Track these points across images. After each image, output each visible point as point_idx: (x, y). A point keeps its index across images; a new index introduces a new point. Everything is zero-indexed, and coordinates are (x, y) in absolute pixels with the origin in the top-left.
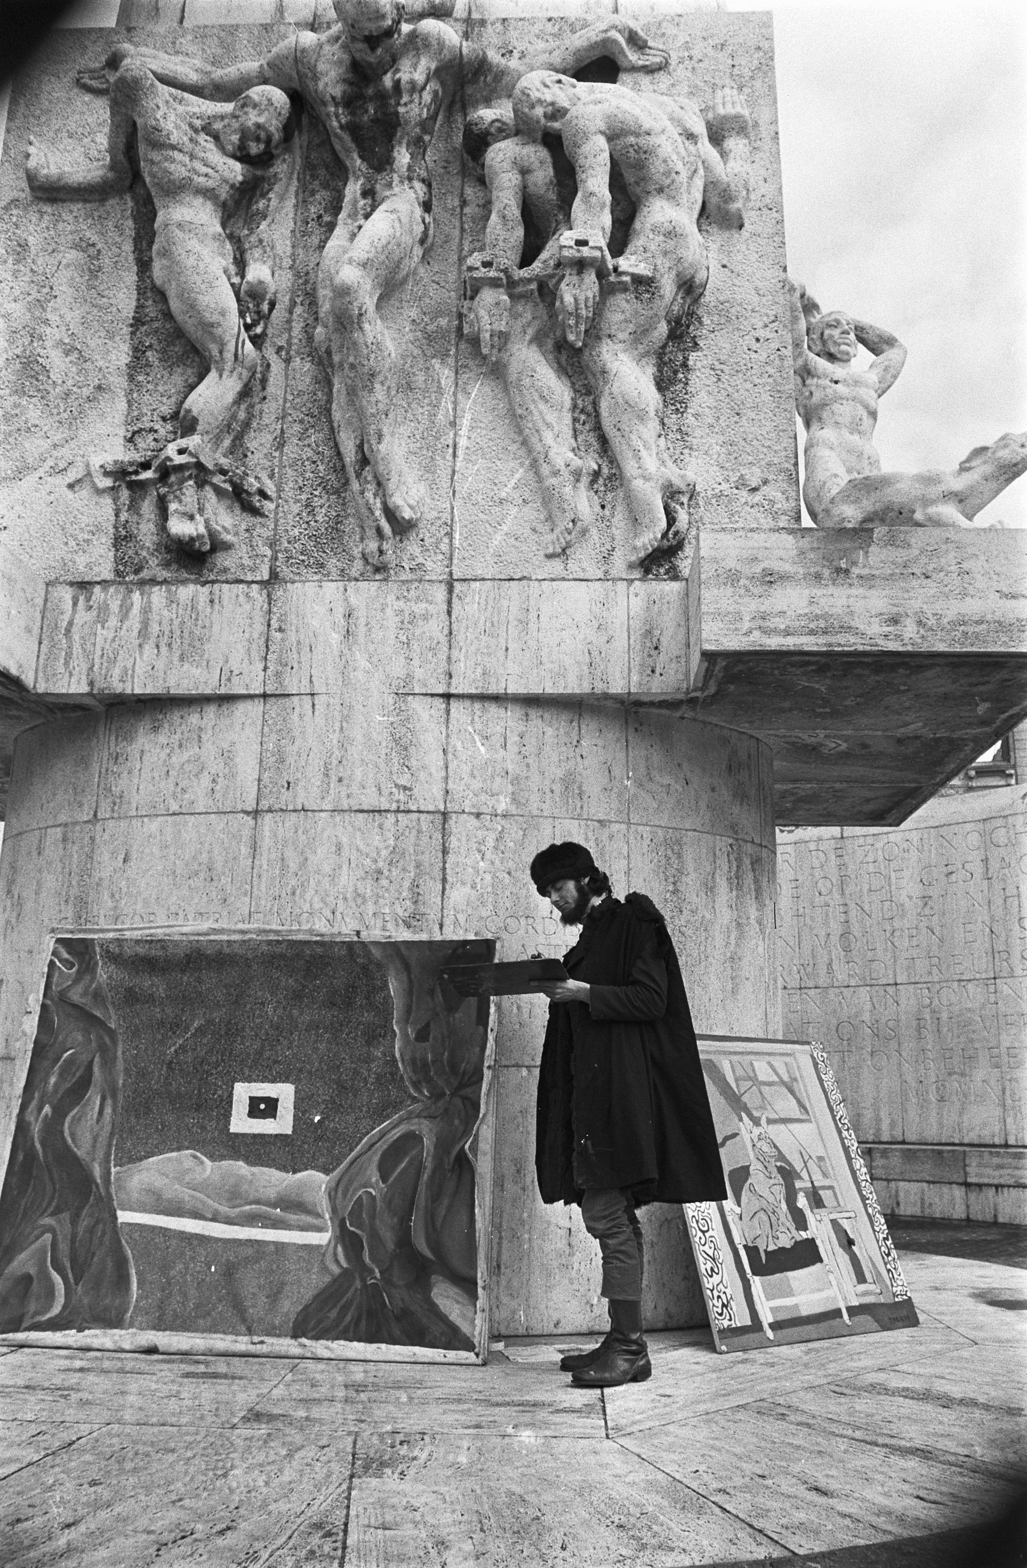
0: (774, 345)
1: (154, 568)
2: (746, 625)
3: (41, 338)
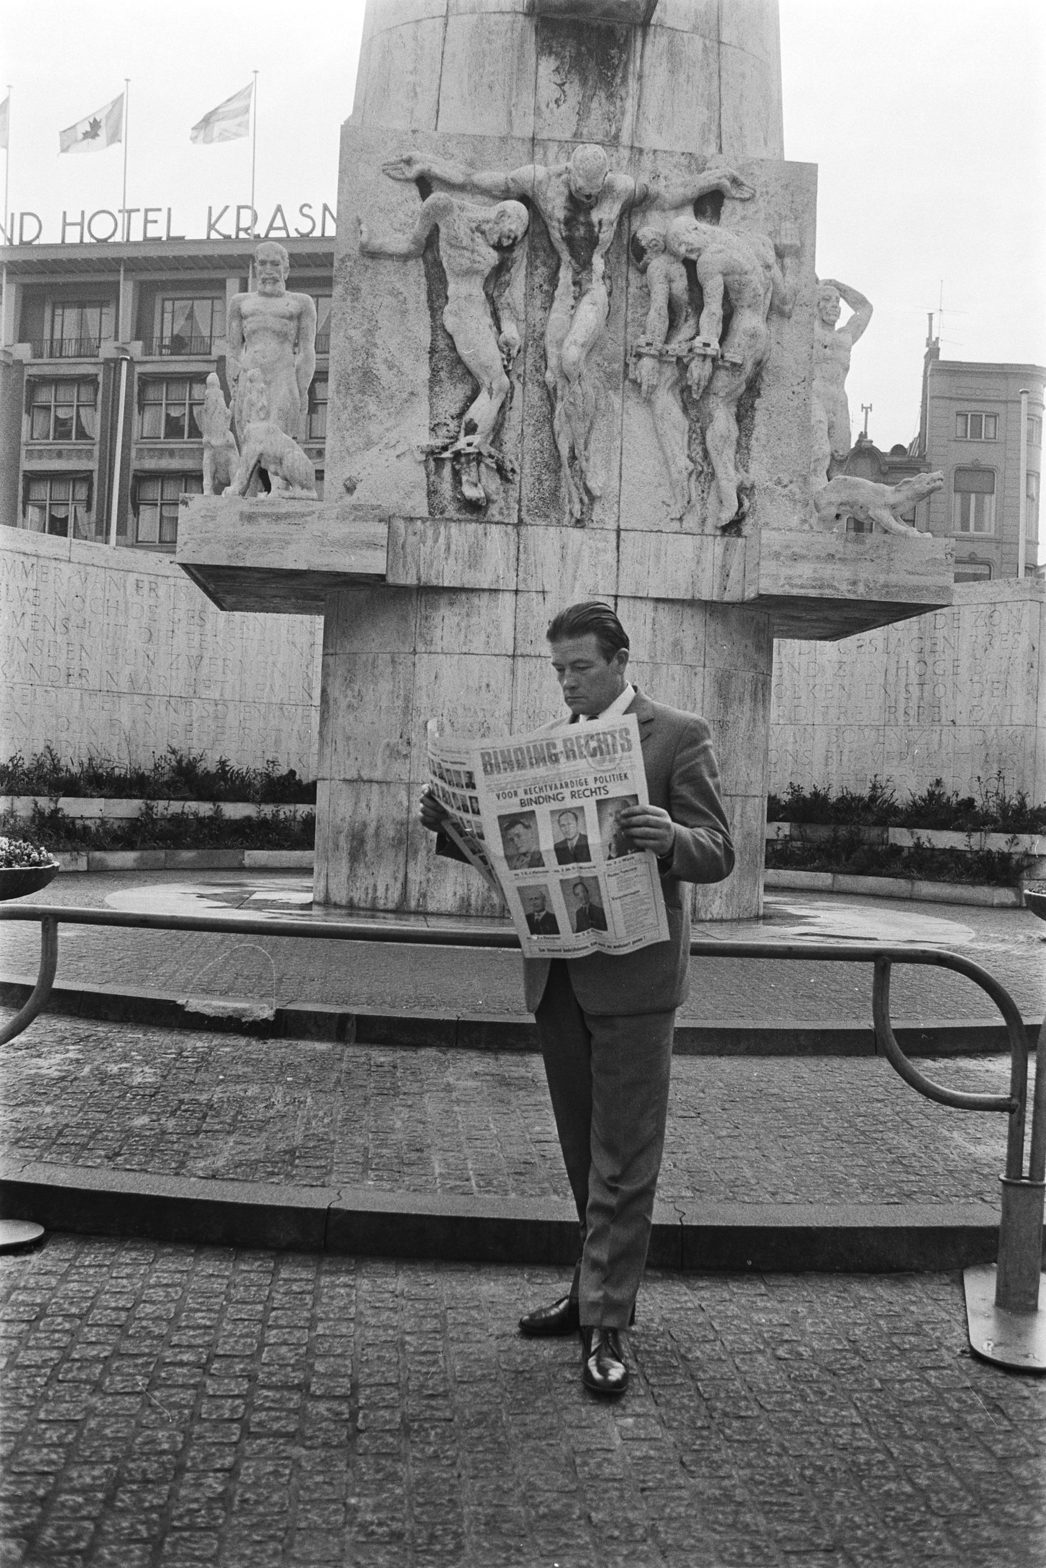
0: (804, 396)
1: (451, 511)
2: (782, 582)
3: (373, 356)
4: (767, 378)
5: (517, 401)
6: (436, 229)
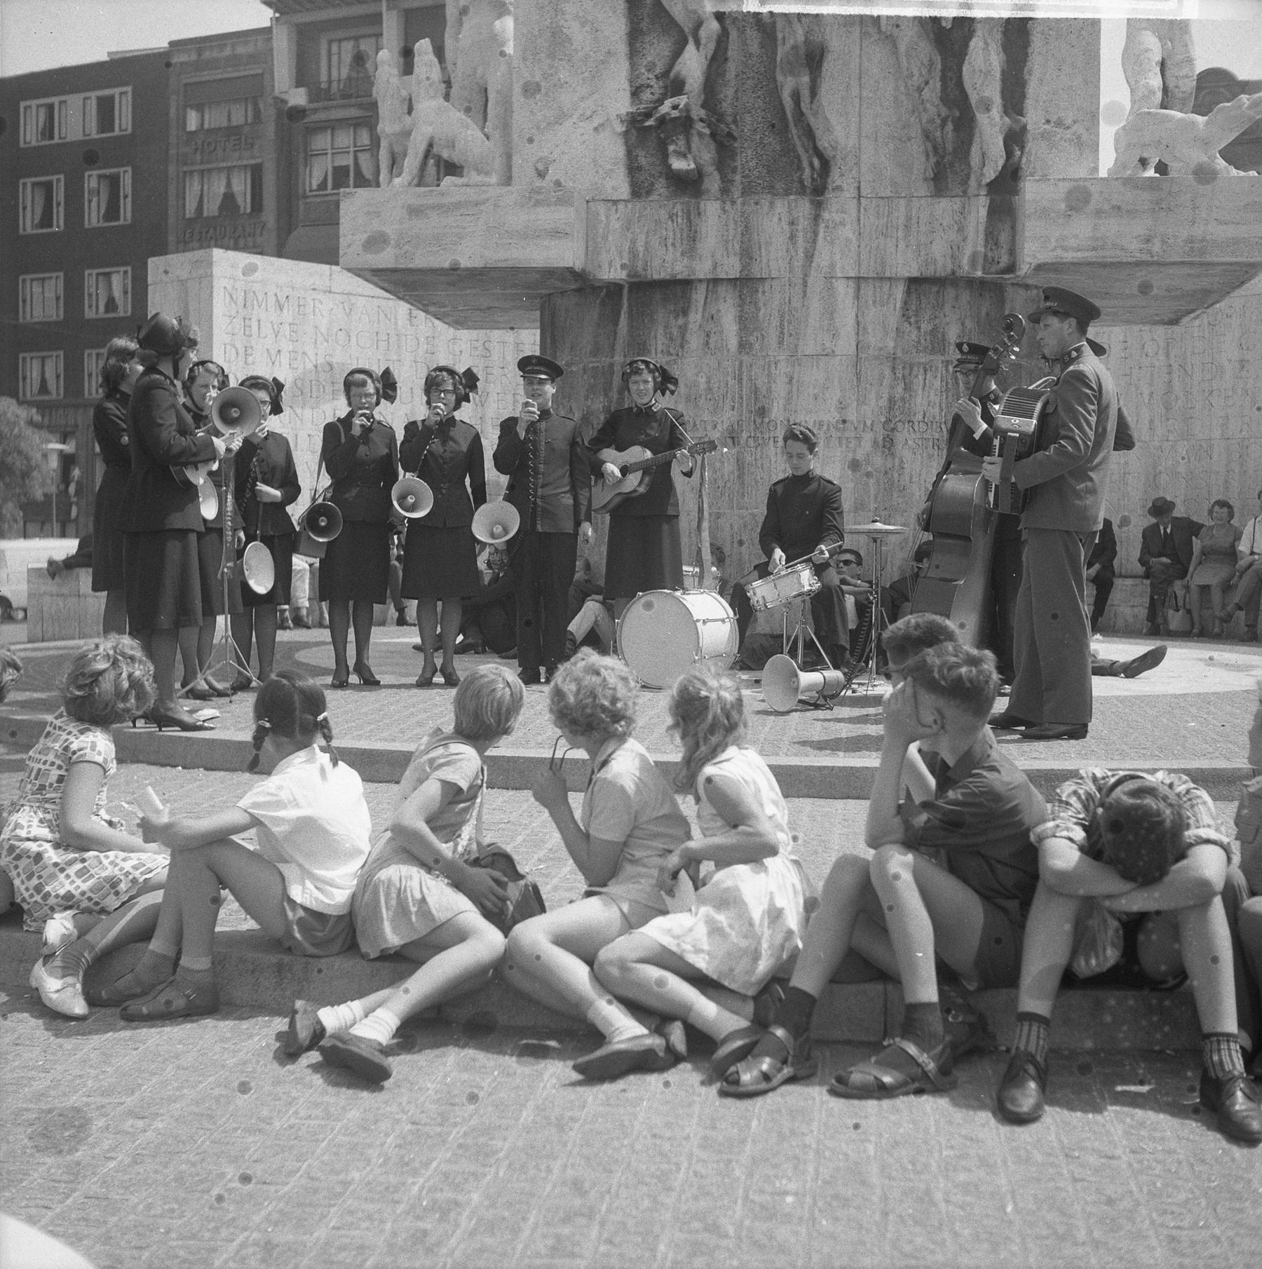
2: (1053, 244)
5: (733, 52)
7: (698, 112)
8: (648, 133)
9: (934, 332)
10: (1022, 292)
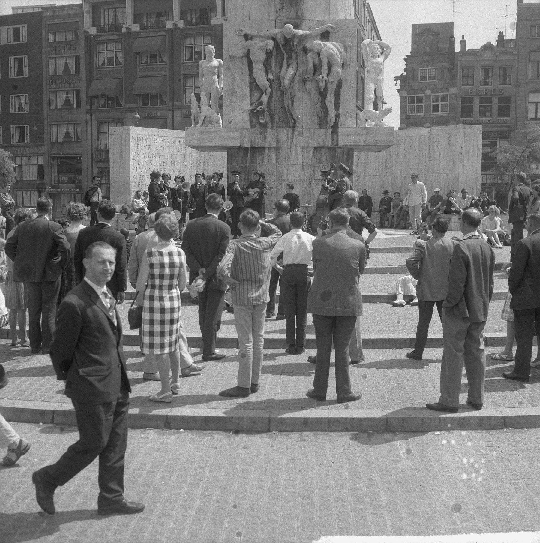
4: (343, 83)
5: (274, 94)
6: (249, 50)
7: (266, 109)
8: (255, 114)
9: (320, 159)
10: (340, 149)
